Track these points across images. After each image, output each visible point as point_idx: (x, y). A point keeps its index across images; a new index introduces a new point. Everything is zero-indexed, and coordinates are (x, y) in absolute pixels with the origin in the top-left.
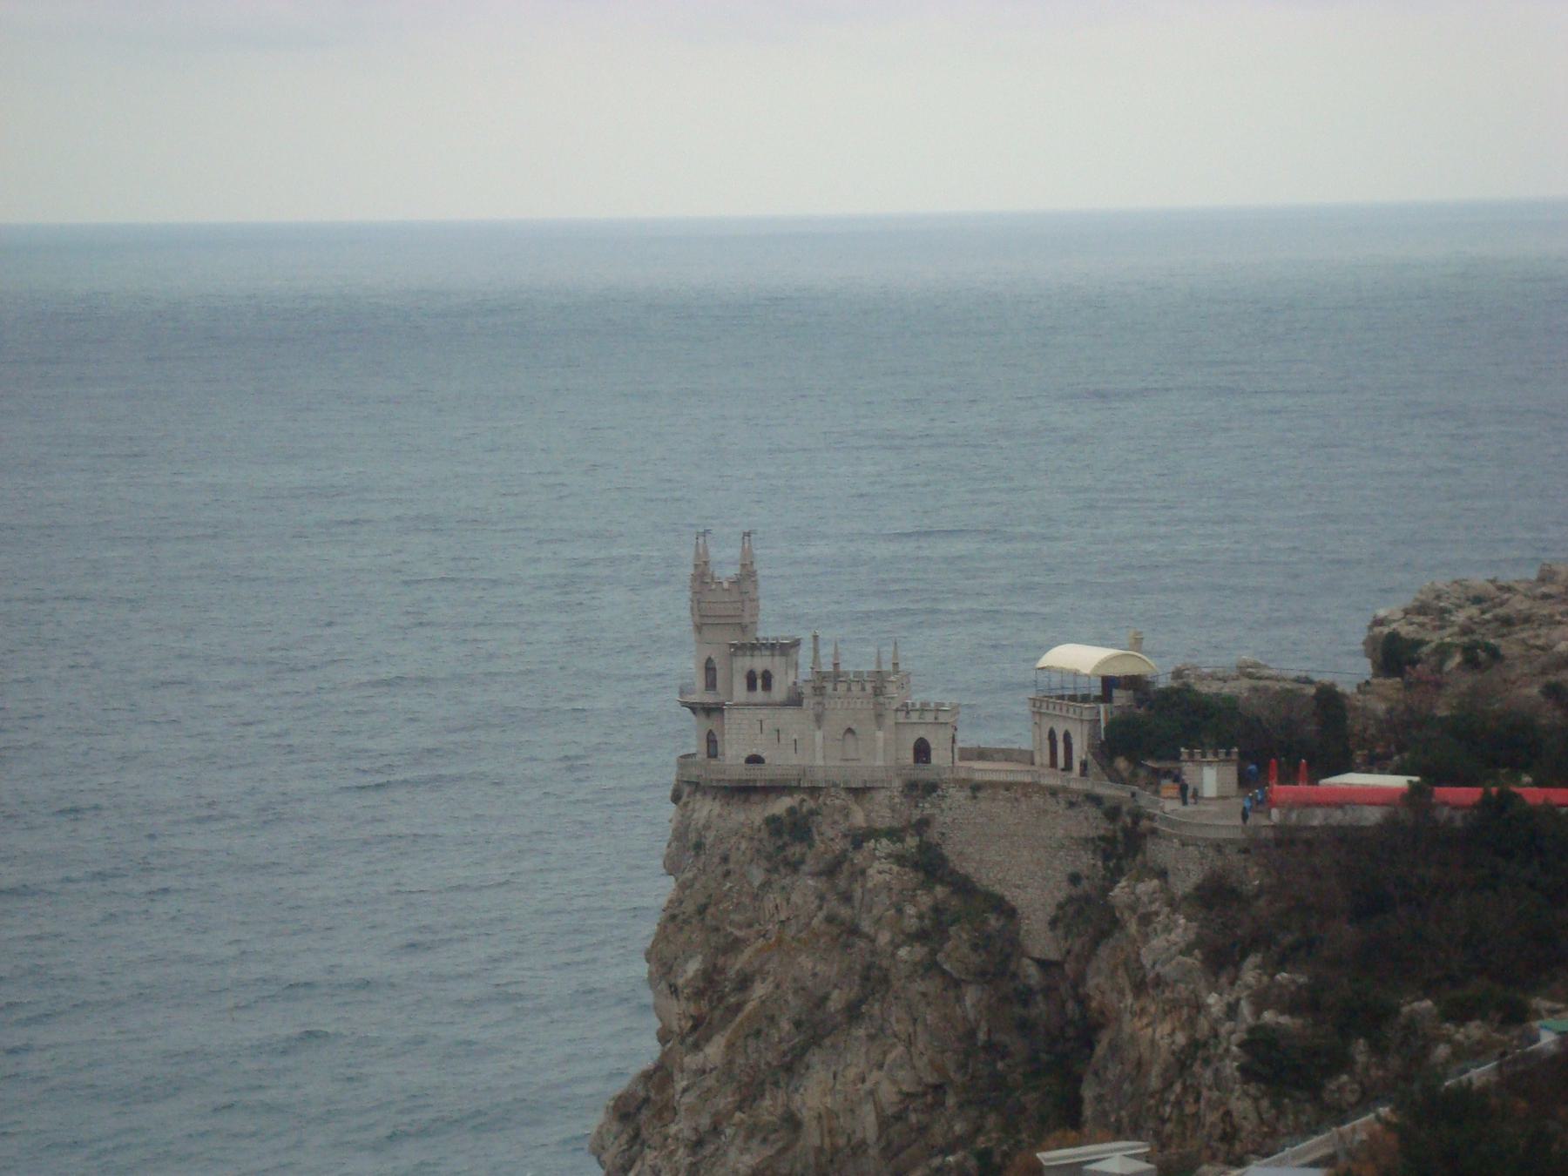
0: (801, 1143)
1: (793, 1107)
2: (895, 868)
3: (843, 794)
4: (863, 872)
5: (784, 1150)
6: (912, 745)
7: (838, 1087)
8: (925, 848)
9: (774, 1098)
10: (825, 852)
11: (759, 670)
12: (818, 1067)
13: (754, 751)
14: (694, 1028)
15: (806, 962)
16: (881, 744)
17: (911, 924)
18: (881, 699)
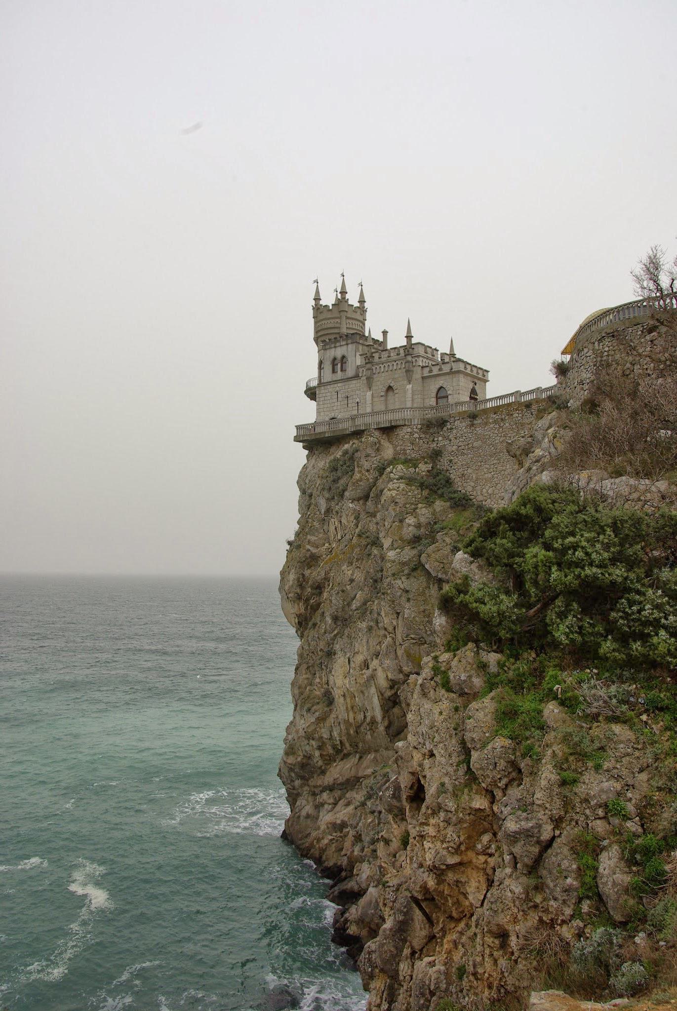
0: (333, 716)
1: (331, 683)
2: (402, 486)
3: (377, 433)
4: (382, 491)
5: (322, 719)
6: (434, 395)
7: (351, 671)
8: (434, 473)
9: (320, 678)
10: (361, 480)
11: (339, 356)
12: (339, 654)
13: (332, 415)
14: (300, 623)
15: (348, 571)
16: (409, 394)
17: (409, 531)
18: (409, 358)
